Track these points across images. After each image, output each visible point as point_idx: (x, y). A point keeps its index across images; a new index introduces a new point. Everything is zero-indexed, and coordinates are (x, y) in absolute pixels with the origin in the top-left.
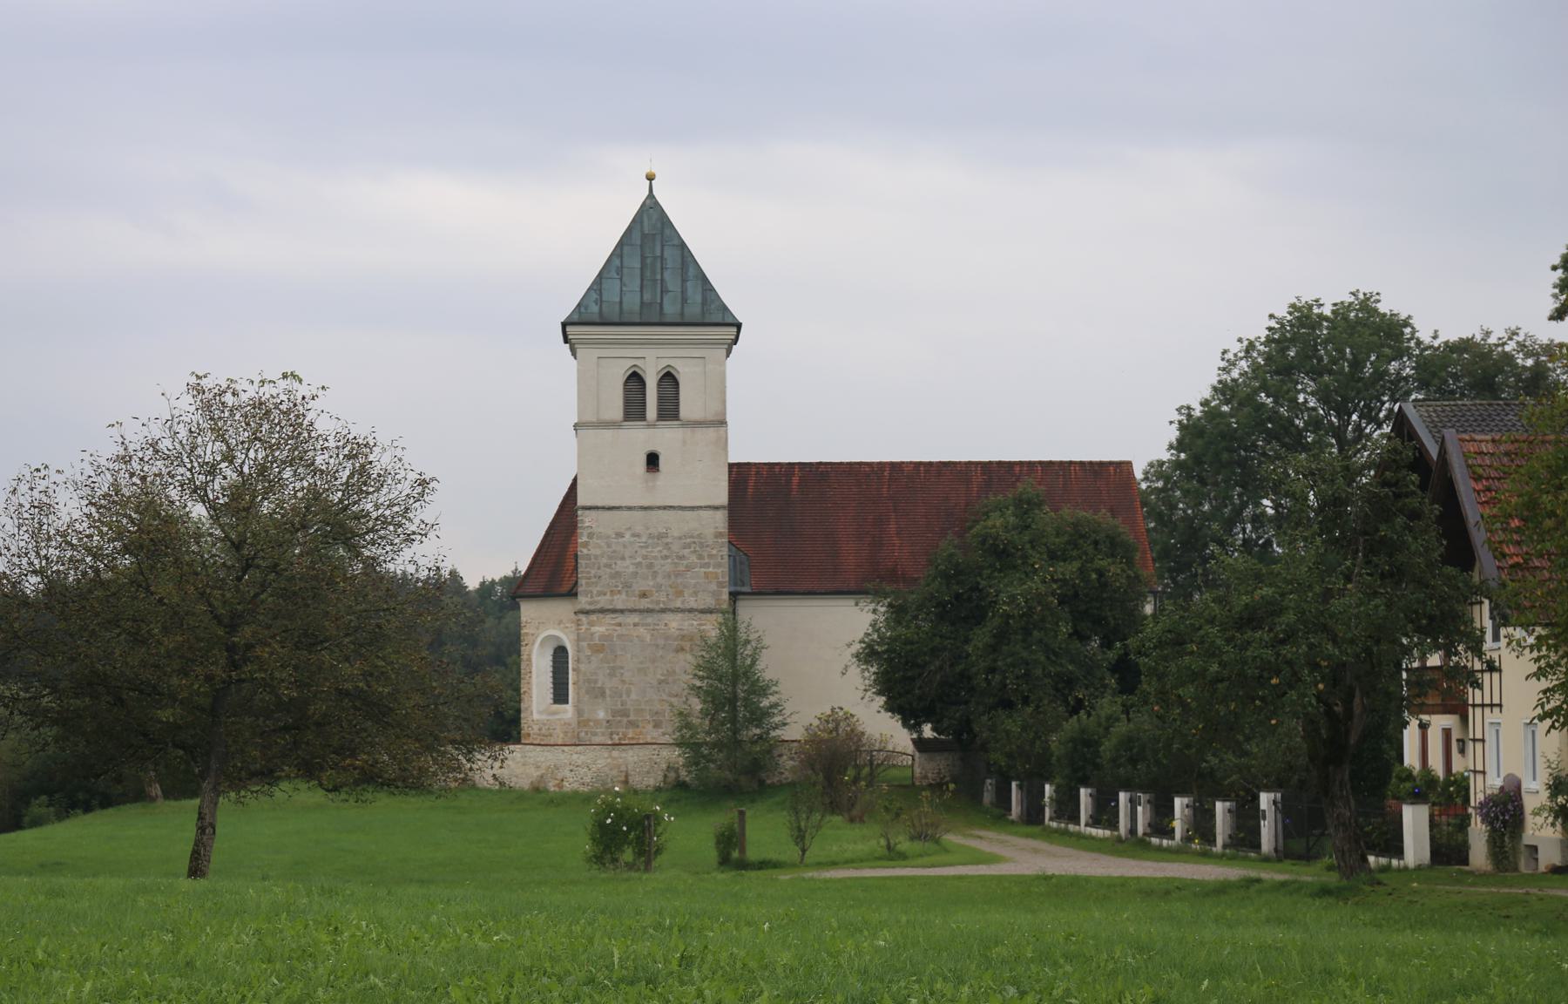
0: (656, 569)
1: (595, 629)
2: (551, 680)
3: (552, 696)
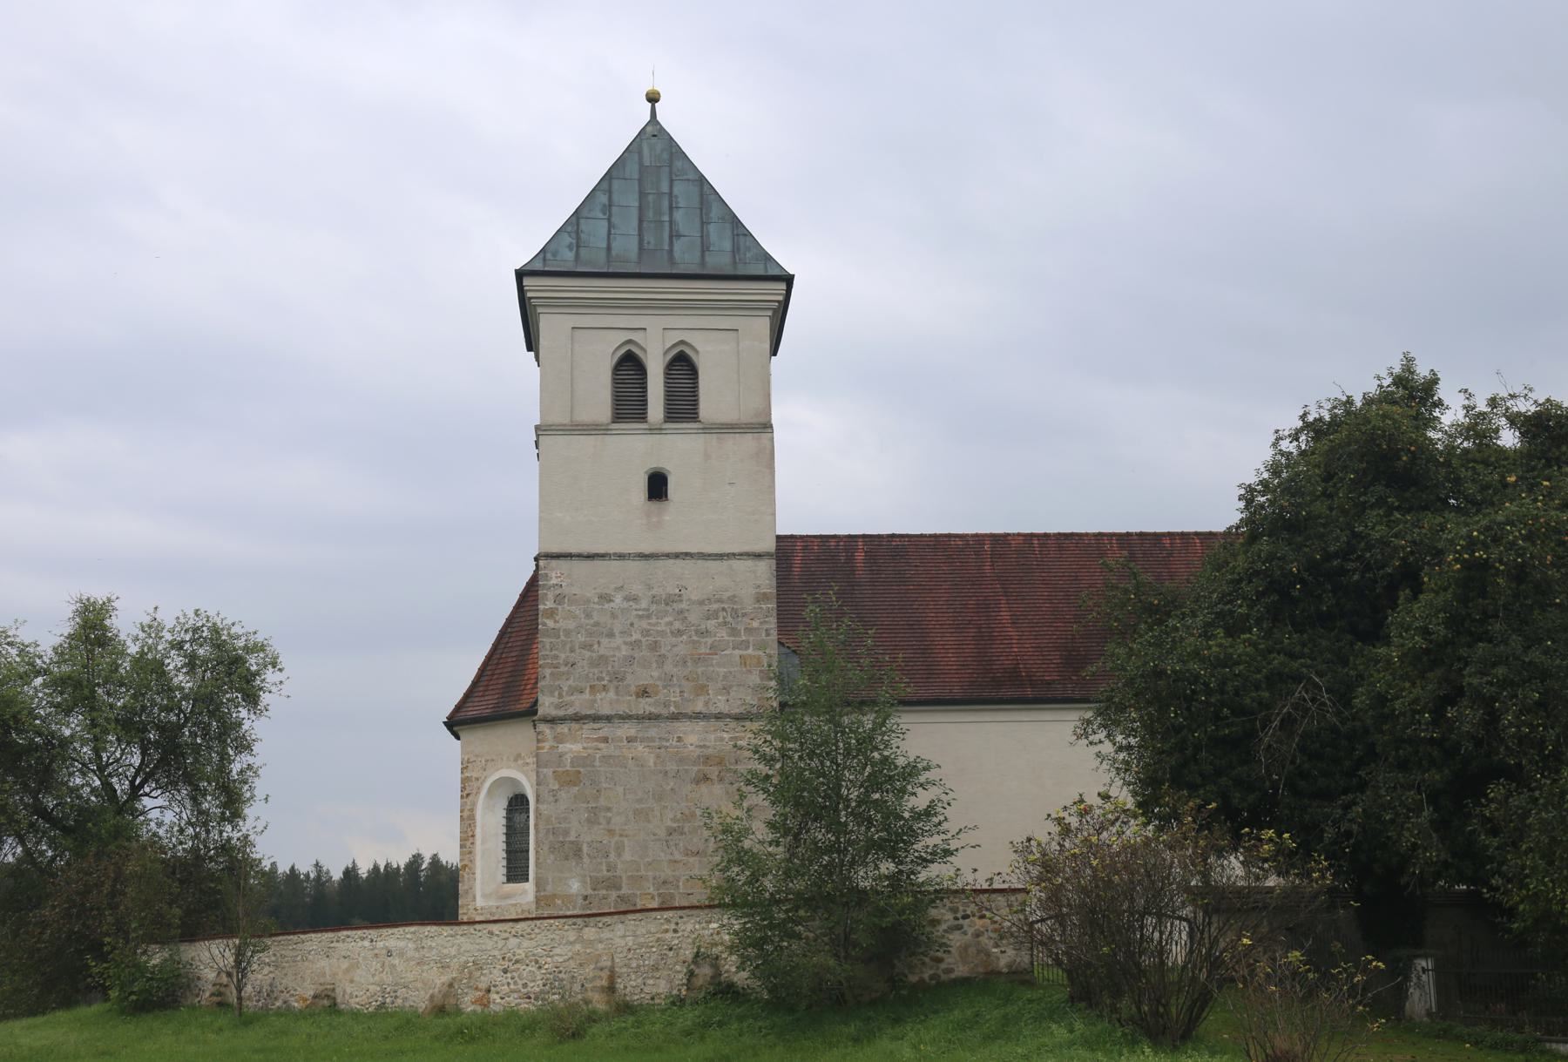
0: (663, 651)
1: (563, 748)
2: (504, 846)
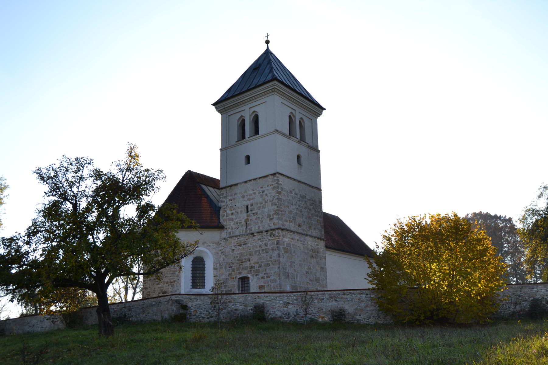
2: (191, 275)
3: (191, 284)
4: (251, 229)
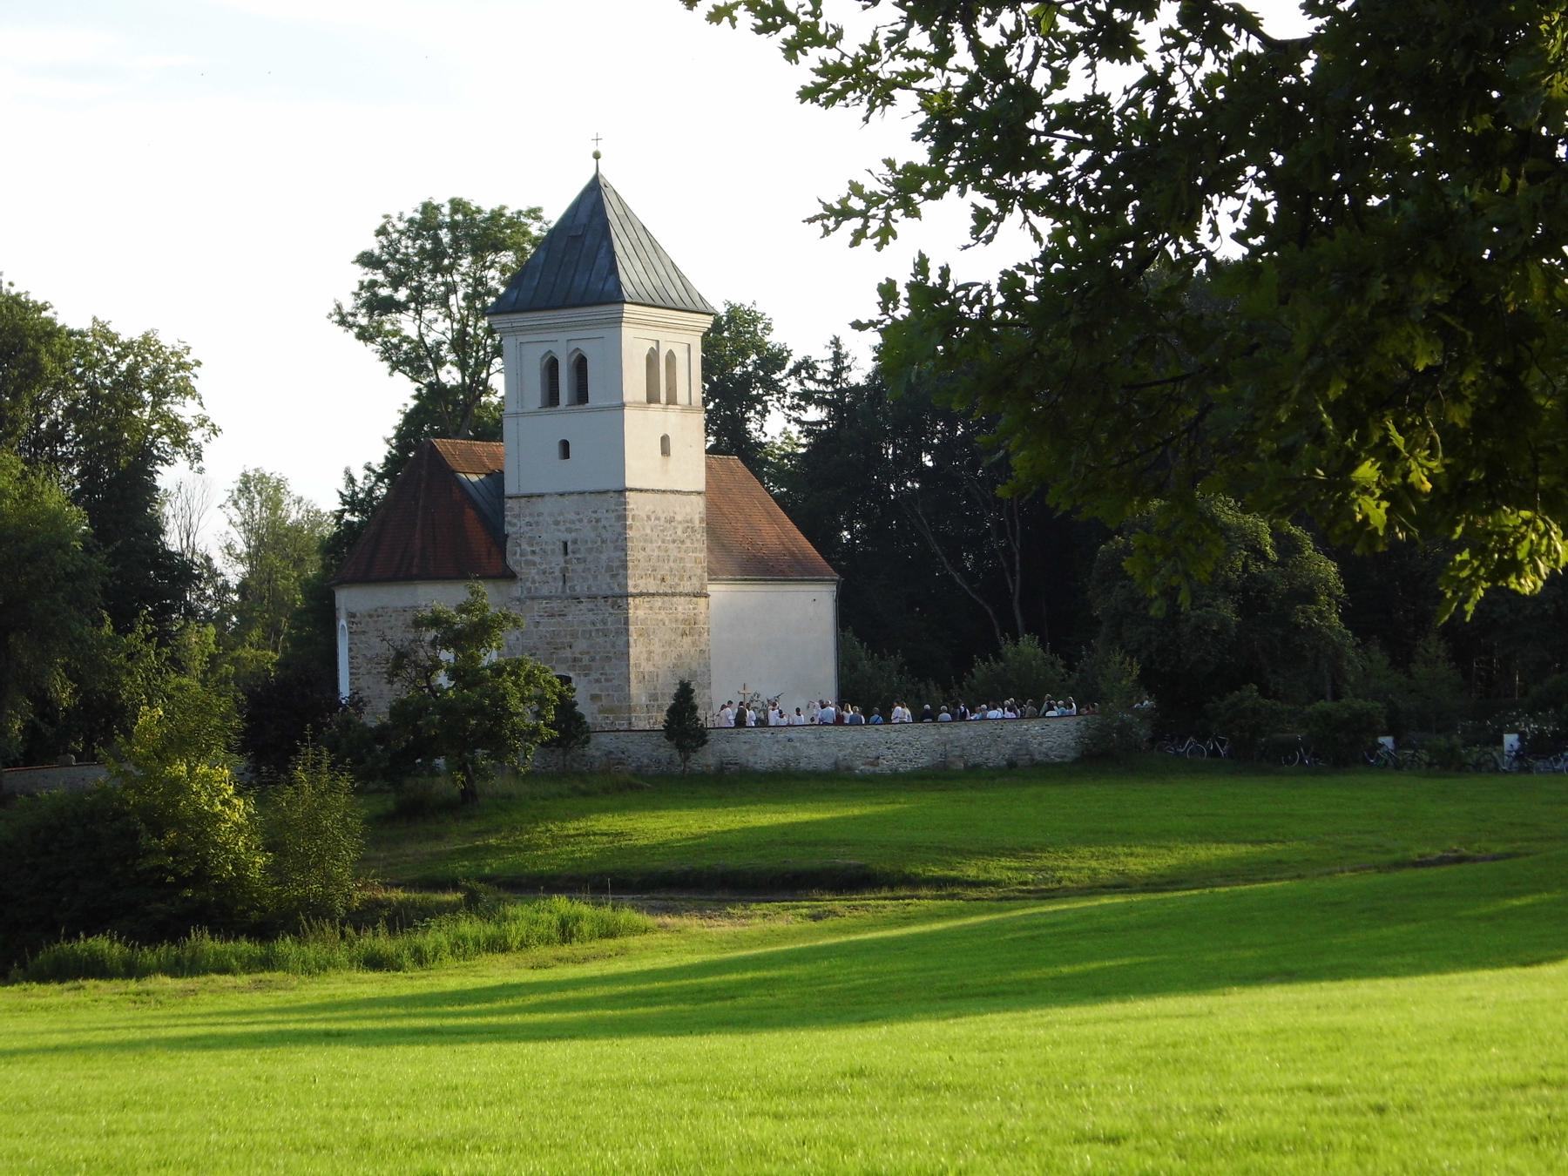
4: (572, 588)
